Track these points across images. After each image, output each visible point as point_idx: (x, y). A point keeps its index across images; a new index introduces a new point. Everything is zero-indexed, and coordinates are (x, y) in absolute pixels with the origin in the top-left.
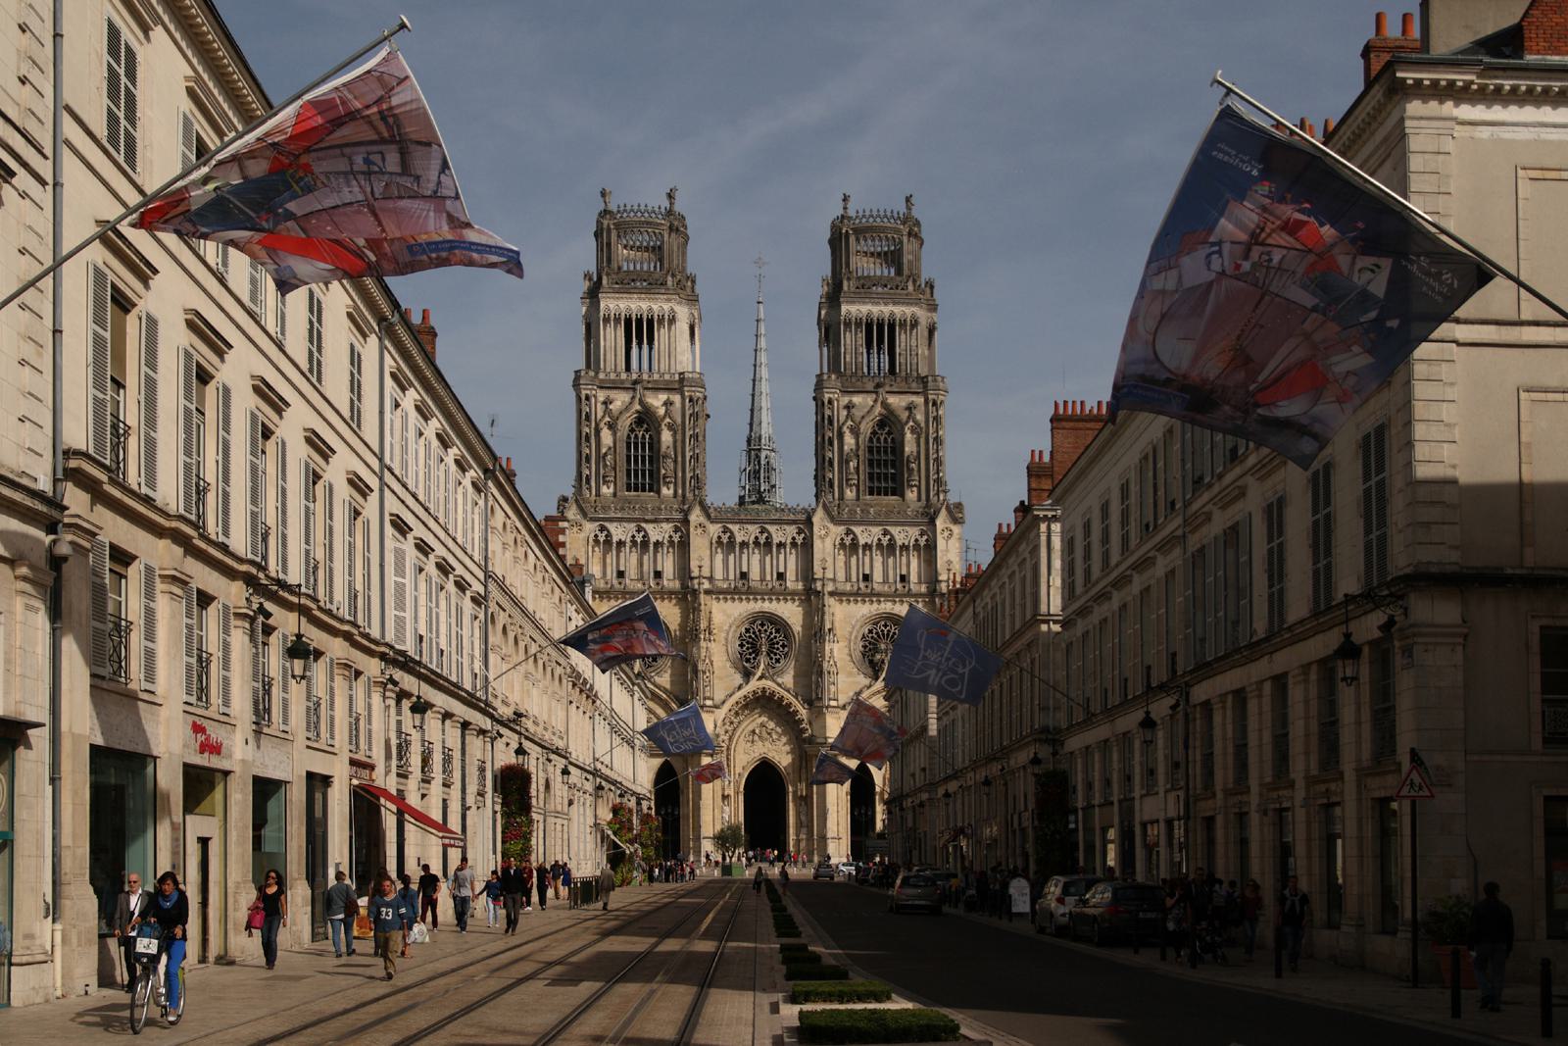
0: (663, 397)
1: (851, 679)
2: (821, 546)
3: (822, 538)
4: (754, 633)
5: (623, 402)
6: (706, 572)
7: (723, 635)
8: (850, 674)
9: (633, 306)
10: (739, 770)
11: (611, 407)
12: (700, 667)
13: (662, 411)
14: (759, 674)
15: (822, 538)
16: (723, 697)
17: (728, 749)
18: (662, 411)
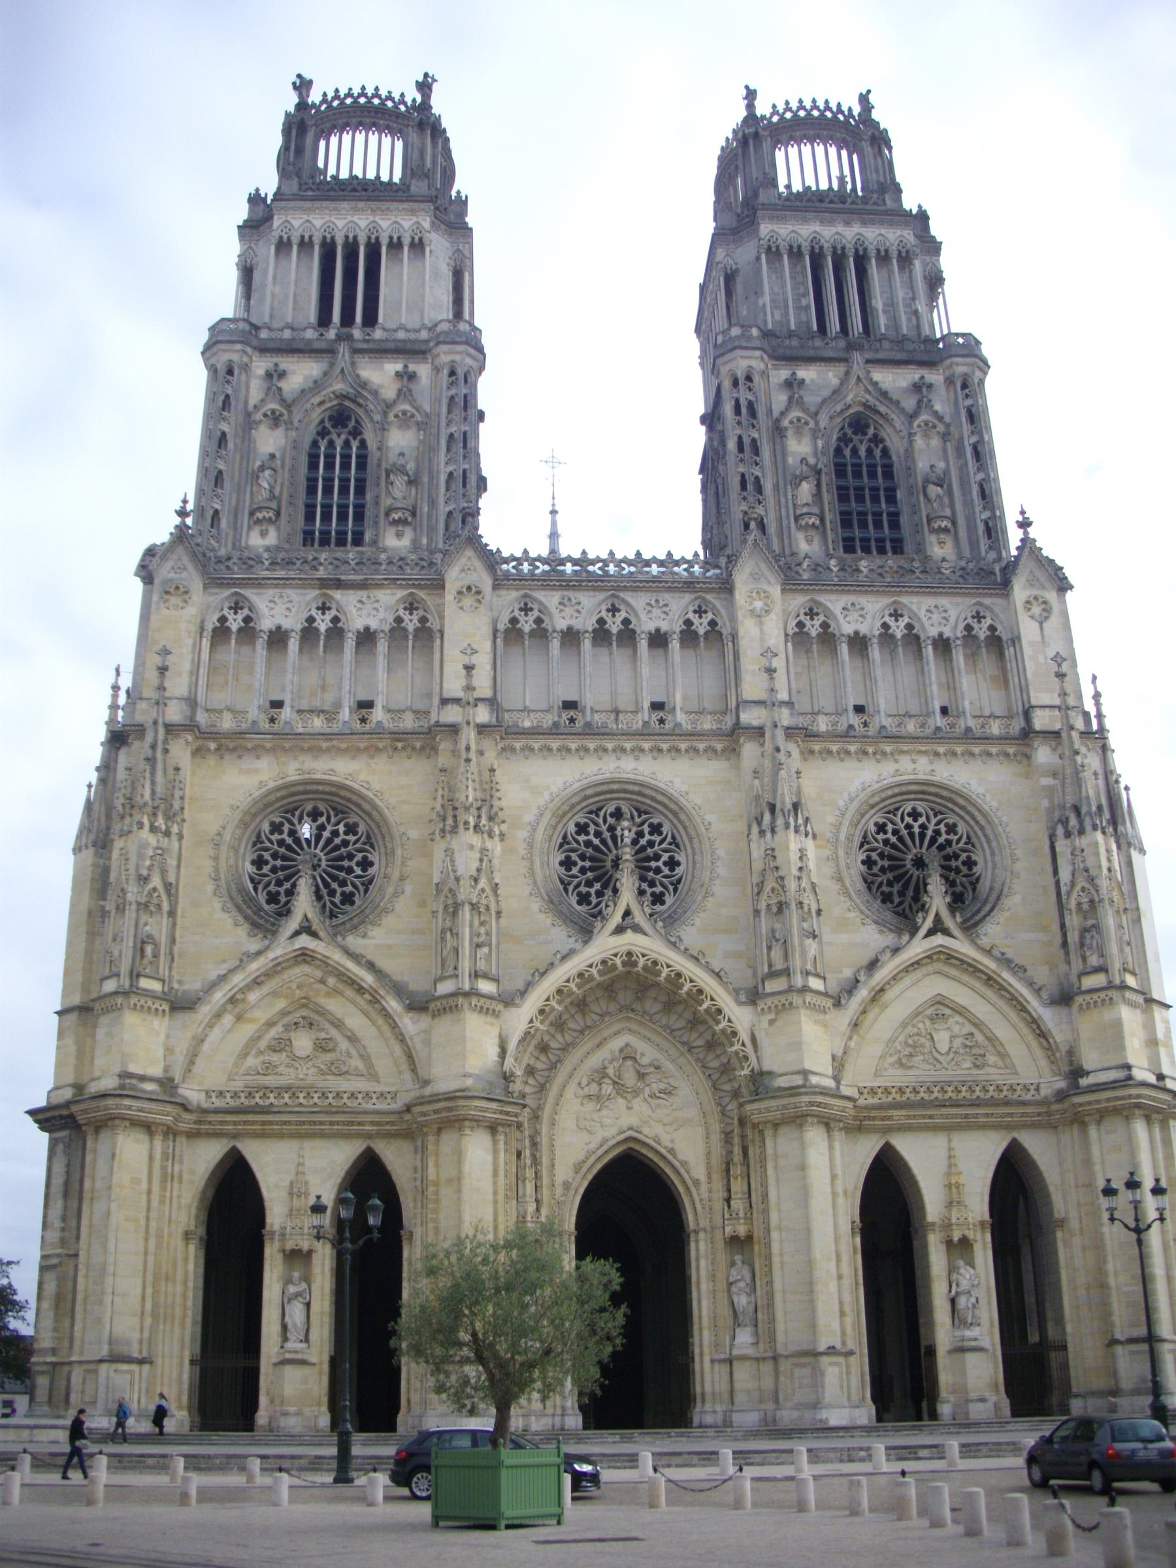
0: (393, 367)
1: (844, 938)
3: (758, 616)
4: (598, 834)
5: (305, 379)
7: (523, 834)
9: (340, 224)
11: (283, 384)
12: (465, 892)
13: (389, 393)
14: (617, 919)
16: (520, 985)
17: (536, 1117)
18: (389, 393)
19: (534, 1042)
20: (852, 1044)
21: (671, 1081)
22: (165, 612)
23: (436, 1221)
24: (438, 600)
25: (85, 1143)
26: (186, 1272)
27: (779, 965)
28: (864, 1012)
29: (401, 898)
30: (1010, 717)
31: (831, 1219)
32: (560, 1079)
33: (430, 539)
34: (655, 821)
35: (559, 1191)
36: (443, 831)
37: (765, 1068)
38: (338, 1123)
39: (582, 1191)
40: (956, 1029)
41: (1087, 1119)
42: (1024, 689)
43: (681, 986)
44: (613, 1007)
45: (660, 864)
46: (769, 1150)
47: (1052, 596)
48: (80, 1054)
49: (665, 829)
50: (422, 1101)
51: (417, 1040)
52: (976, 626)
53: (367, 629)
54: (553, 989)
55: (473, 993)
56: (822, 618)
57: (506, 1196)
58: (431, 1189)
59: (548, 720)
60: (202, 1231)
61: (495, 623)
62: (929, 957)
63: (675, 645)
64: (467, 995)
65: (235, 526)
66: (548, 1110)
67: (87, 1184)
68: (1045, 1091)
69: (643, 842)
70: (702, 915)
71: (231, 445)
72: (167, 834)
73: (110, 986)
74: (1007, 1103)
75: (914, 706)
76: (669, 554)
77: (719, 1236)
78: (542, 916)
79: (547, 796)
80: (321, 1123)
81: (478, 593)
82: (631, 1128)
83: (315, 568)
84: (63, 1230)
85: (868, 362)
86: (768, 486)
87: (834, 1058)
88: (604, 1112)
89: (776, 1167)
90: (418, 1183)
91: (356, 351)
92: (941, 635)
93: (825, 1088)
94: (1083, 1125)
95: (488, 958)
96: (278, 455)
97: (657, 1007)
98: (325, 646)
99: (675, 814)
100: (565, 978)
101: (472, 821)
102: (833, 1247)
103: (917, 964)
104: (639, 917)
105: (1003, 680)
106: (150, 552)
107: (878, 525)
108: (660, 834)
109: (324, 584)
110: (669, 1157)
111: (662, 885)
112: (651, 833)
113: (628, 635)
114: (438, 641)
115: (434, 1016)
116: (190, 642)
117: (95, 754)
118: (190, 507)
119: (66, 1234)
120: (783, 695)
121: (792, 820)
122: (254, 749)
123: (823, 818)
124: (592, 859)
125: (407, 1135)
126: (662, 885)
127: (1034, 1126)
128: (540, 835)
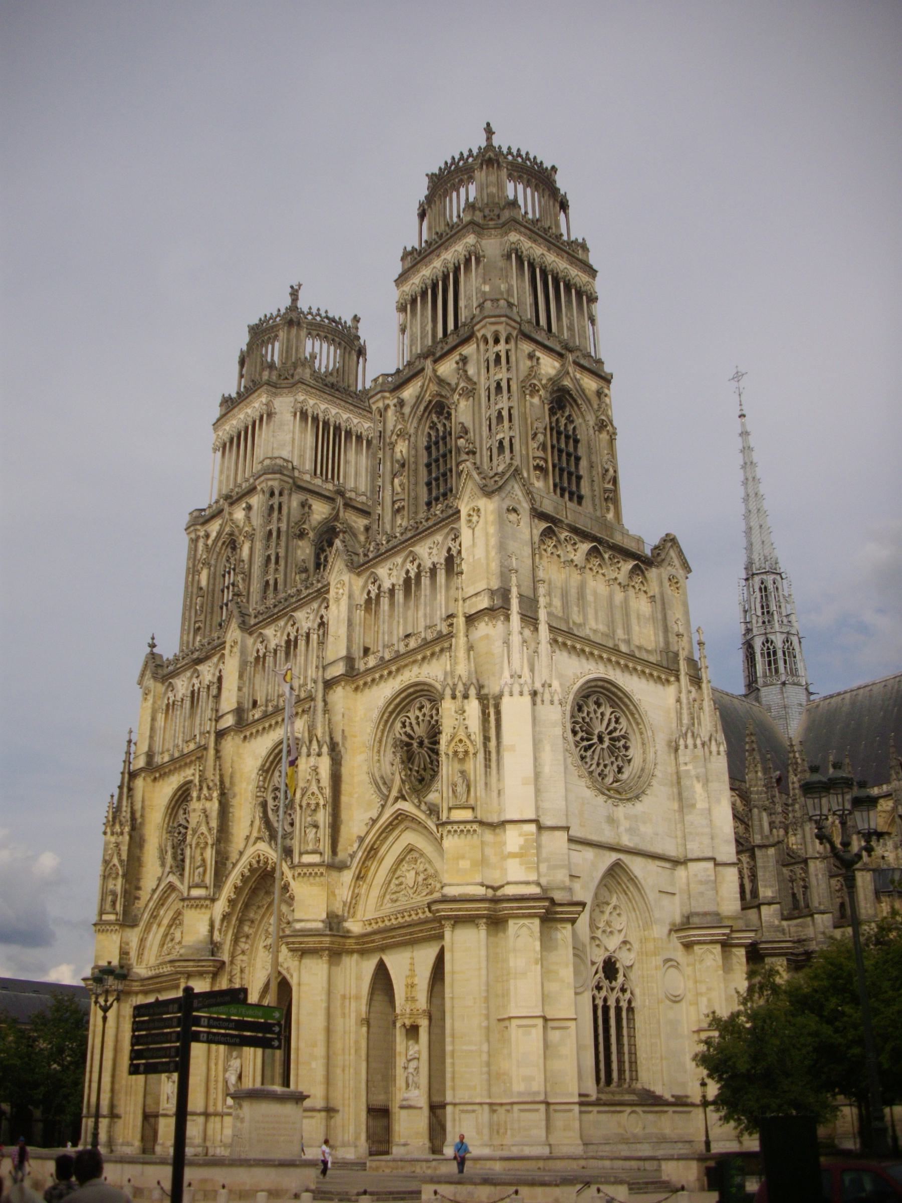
15: (337, 600)
62: (396, 818)
72: (122, 833)
85: (435, 361)
91: (231, 504)
93: (311, 930)
103: (391, 827)
122: (170, 771)
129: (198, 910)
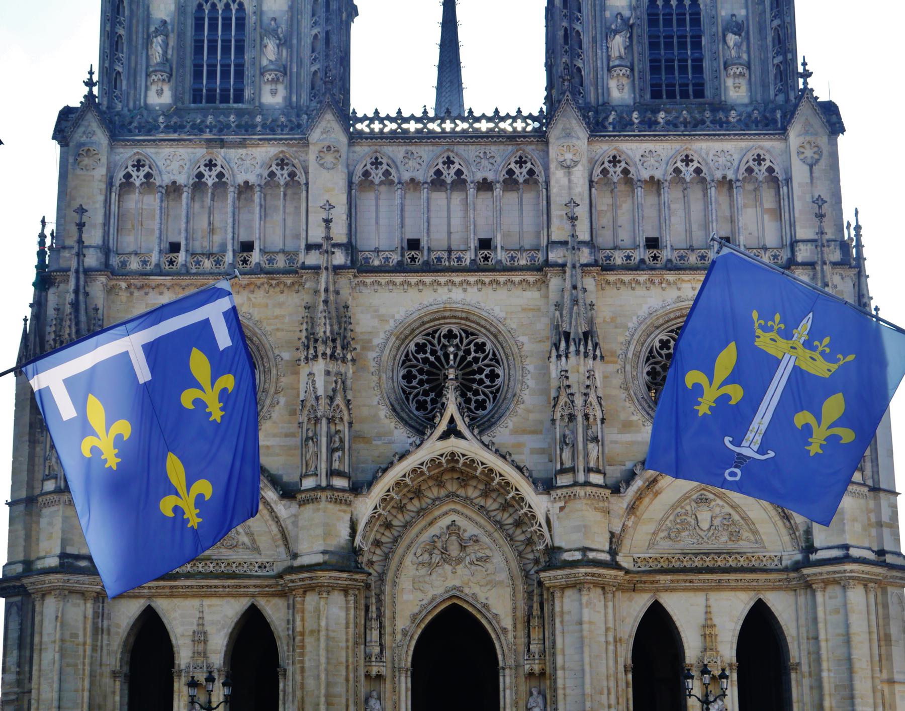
1: (628, 437)
2: (564, 181)
3: (568, 168)
4: (433, 353)
6: (339, 233)
7: (372, 355)
8: (627, 426)
10: (402, 623)
12: (323, 408)
14: (443, 426)
15: (568, 168)
16: (369, 477)
17: (381, 578)
19: (378, 524)
20: (630, 523)
21: (488, 552)
22: (78, 172)
23: (302, 662)
24: (303, 157)
25: (34, 606)
26: (114, 702)
27: (568, 464)
28: (639, 497)
29: (277, 408)
30: (783, 246)
31: (604, 661)
32: (400, 551)
33: (299, 96)
34: (480, 341)
35: (399, 637)
36: (307, 358)
37: (556, 544)
38: (229, 586)
39: (416, 637)
40: (717, 510)
41: (814, 586)
42: (792, 225)
43: (493, 479)
44: (443, 492)
45: (483, 376)
46: (557, 609)
47: (823, 141)
48: (28, 537)
49: (488, 347)
50: (291, 570)
51: (289, 522)
52: (756, 168)
53: (246, 183)
54: (393, 482)
55: (330, 487)
56: (623, 165)
57: (356, 644)
58: (298, 638)
59: (395, 258)
60: (126, 669)
61: (350, 175)
63: (498, 191)
64: (323, 489)
65: (134, 84)
66: (390, 575)
67: (36, 639)
68: (786, 562)
69: (470, 358)
70: (514, 419)
71: (127, 13)
73: (50, 486)
74: (753, 570)
75: (698, 237)
76: (497, 112)
77: (521, 673)
78: (387, 421)
79: (392, 323)
80: (216, 587)
81: (338, 151)
82: (455, 588)
83: (201, 131)
84: (18, 673)
86: (586, 40)
87: (612, 535)
88: (434, 576)
89: (562, 622)
90: (291, 632)
92: (724, 177)
94: (814, 592)
95: (341, 459)
96: (168, 19)
97: (477, 493)
98: (213, 194)
99: (495, 336)
100: (402, 474)
101: (329, 352)
102: (605, 684)
104: (461, 426)
105: (778, 213)
106: (66, 114)
107: (683, 69)
108: (484, 351)
109: (209, 143)
110: (483, 610)
111: (484, 394)
112: (476, 352)
113: (460, 182)
114: (304, 193)
115: (300, 505)
116: (101, 198)
117: (28, 294)
118: (95, 78)
119: (22, 677)
120: (584, 236)
121: (582, 348)
123: (613, 339)
124: (428, 373)
125: (283, 594)
126: (484, 394)
127: (774, 589)
128: (385, 358)
129: (338, 507)
